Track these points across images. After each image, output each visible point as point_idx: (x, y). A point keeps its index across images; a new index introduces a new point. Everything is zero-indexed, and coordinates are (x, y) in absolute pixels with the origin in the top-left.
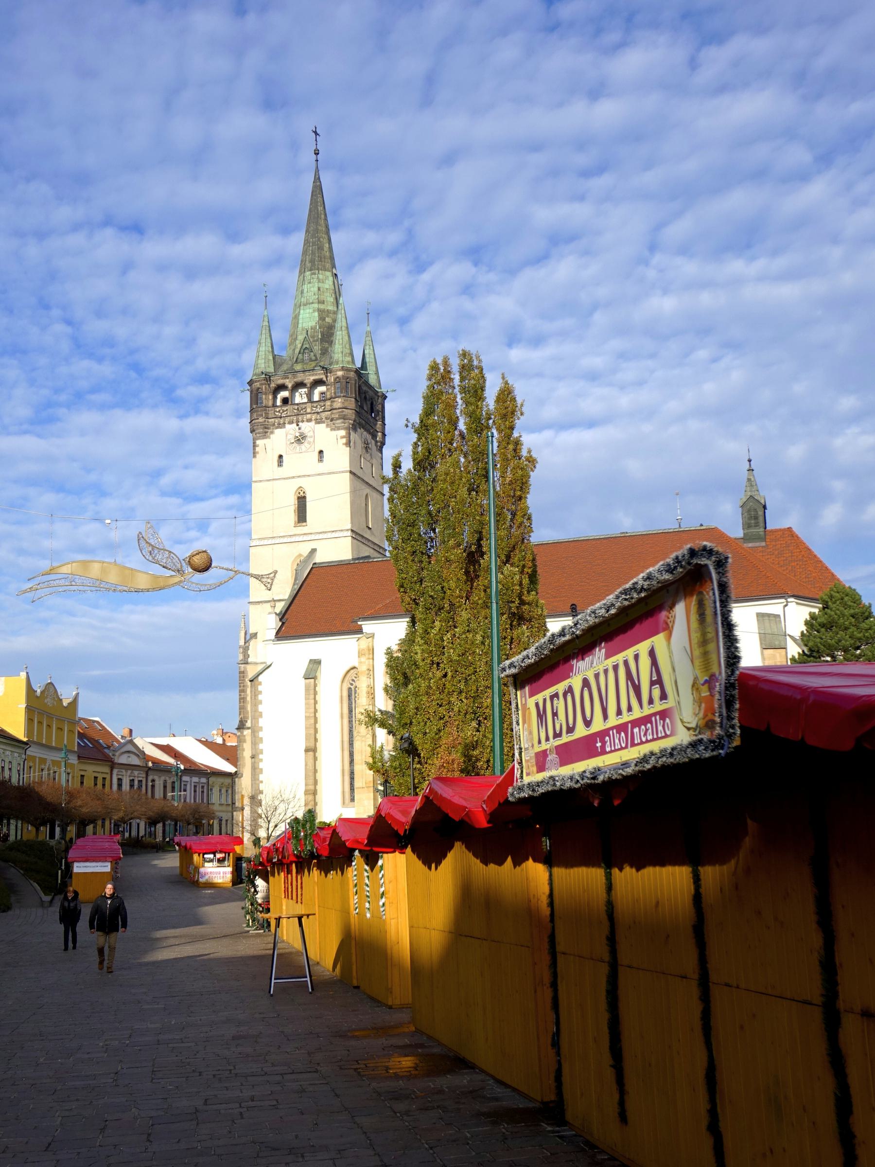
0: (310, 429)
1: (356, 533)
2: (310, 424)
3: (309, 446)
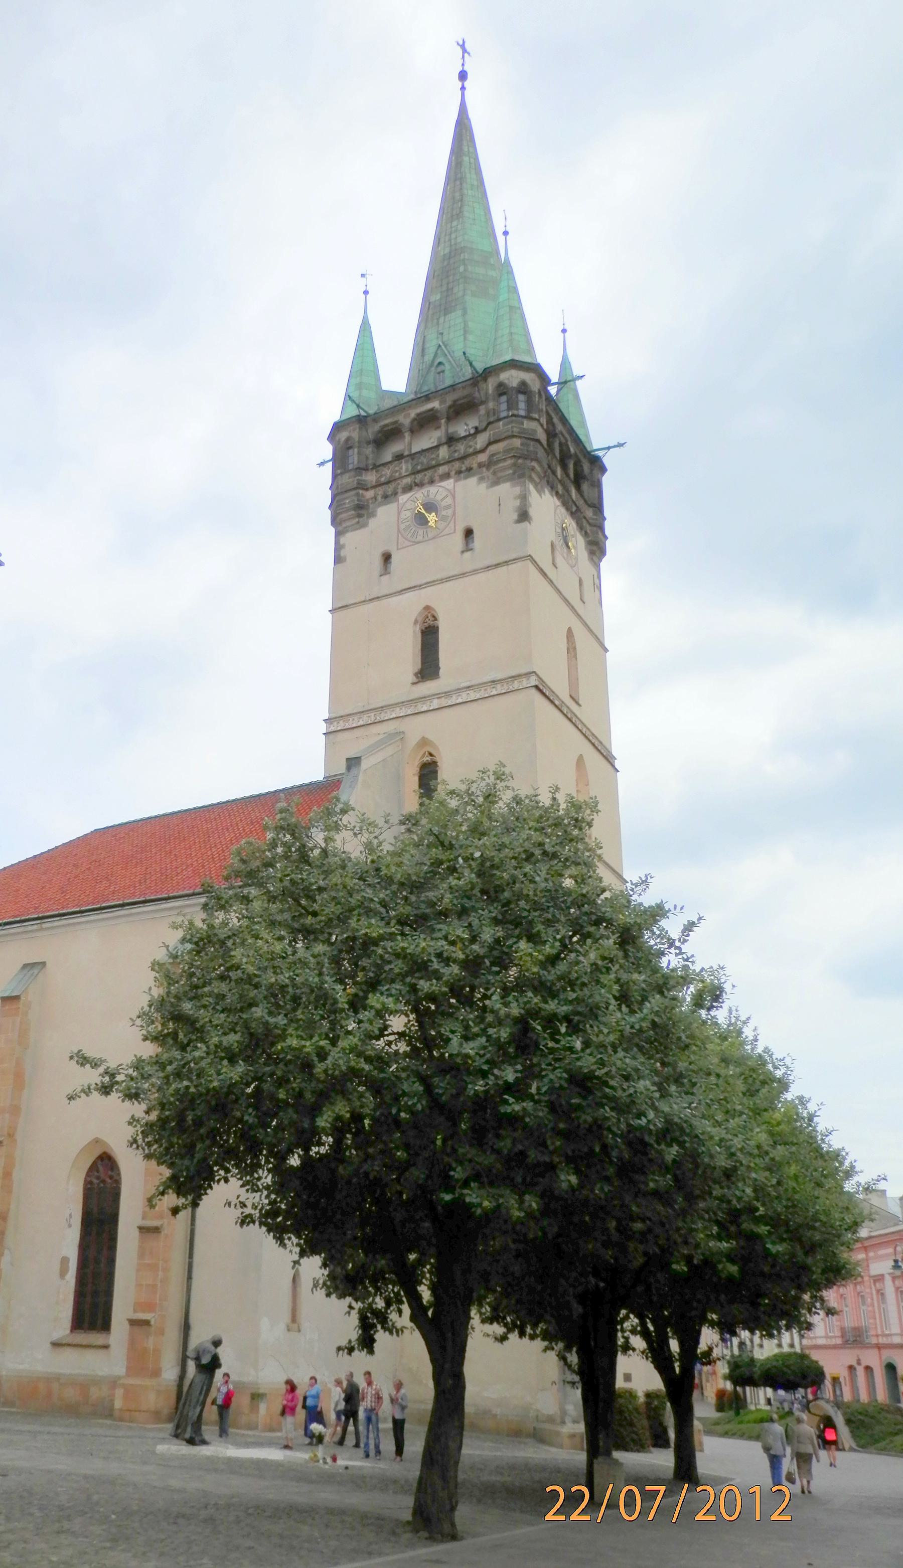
0: (445, 493)
2: (444, 484)
3: (444, 524)
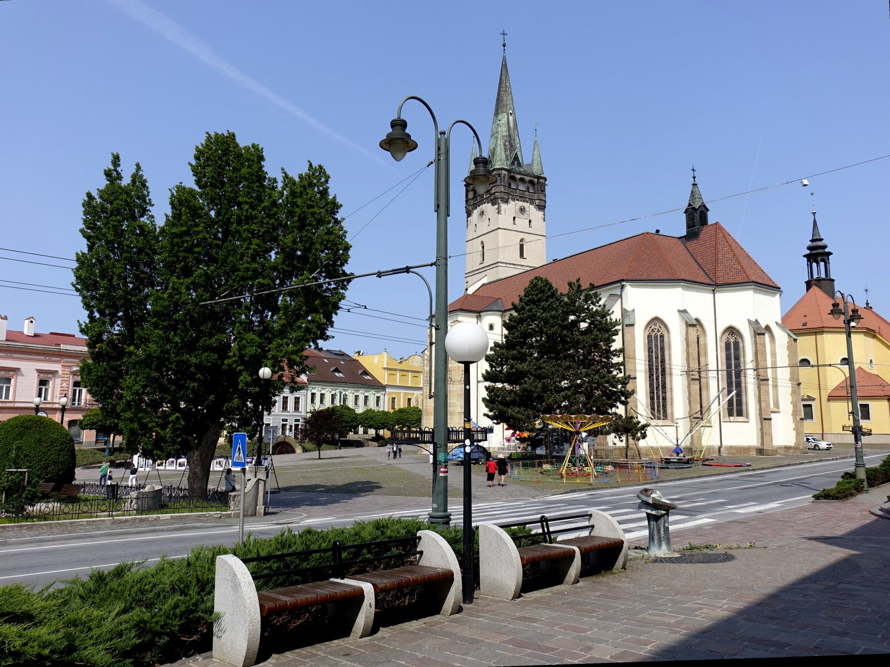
1: (506, 263)
